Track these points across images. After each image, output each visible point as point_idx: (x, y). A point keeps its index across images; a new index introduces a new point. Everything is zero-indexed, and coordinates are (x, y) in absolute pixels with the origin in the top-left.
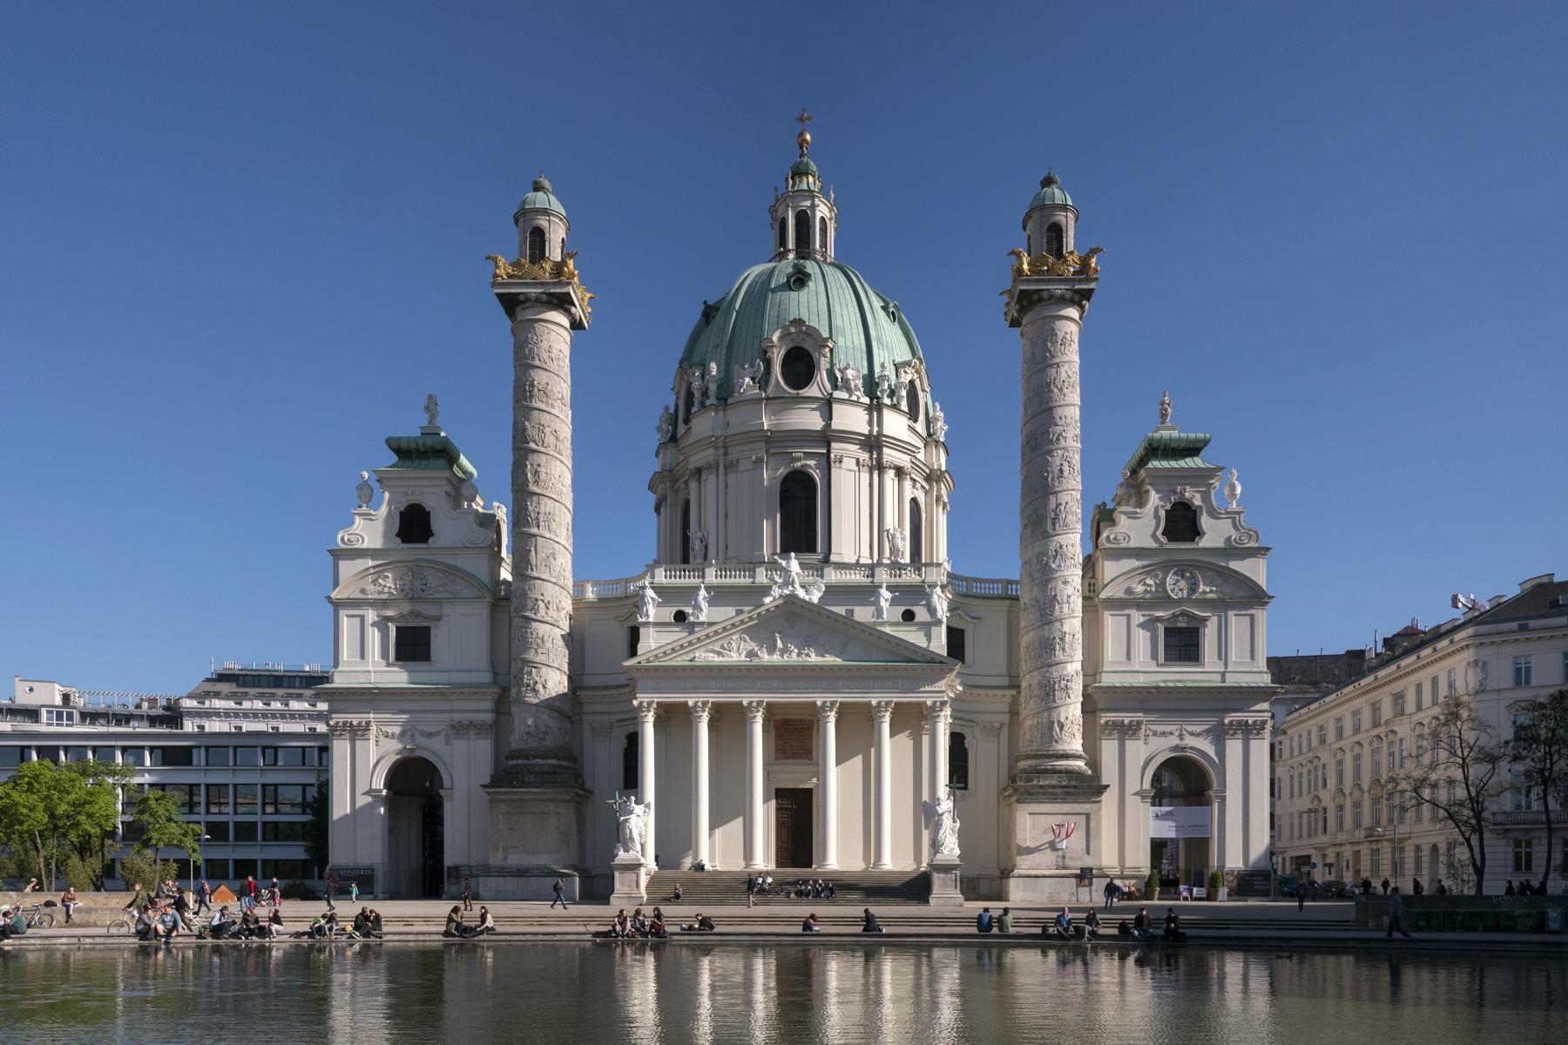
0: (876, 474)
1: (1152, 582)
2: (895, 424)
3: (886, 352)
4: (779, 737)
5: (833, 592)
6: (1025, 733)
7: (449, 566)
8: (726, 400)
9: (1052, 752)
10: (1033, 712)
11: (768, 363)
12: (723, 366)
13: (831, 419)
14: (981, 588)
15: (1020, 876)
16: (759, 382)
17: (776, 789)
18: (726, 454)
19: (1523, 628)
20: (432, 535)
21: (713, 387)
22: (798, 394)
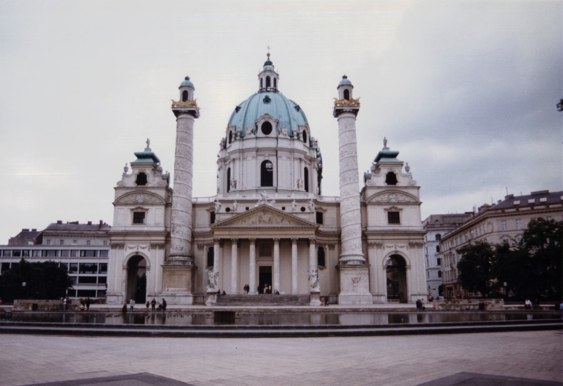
2: (299, 145)
5: (278, 201)
8: (243, 137)
11: (257, 127)
12: (242, 127)
13: (277, 143)
18: (243, 155)
21: (239, 134)
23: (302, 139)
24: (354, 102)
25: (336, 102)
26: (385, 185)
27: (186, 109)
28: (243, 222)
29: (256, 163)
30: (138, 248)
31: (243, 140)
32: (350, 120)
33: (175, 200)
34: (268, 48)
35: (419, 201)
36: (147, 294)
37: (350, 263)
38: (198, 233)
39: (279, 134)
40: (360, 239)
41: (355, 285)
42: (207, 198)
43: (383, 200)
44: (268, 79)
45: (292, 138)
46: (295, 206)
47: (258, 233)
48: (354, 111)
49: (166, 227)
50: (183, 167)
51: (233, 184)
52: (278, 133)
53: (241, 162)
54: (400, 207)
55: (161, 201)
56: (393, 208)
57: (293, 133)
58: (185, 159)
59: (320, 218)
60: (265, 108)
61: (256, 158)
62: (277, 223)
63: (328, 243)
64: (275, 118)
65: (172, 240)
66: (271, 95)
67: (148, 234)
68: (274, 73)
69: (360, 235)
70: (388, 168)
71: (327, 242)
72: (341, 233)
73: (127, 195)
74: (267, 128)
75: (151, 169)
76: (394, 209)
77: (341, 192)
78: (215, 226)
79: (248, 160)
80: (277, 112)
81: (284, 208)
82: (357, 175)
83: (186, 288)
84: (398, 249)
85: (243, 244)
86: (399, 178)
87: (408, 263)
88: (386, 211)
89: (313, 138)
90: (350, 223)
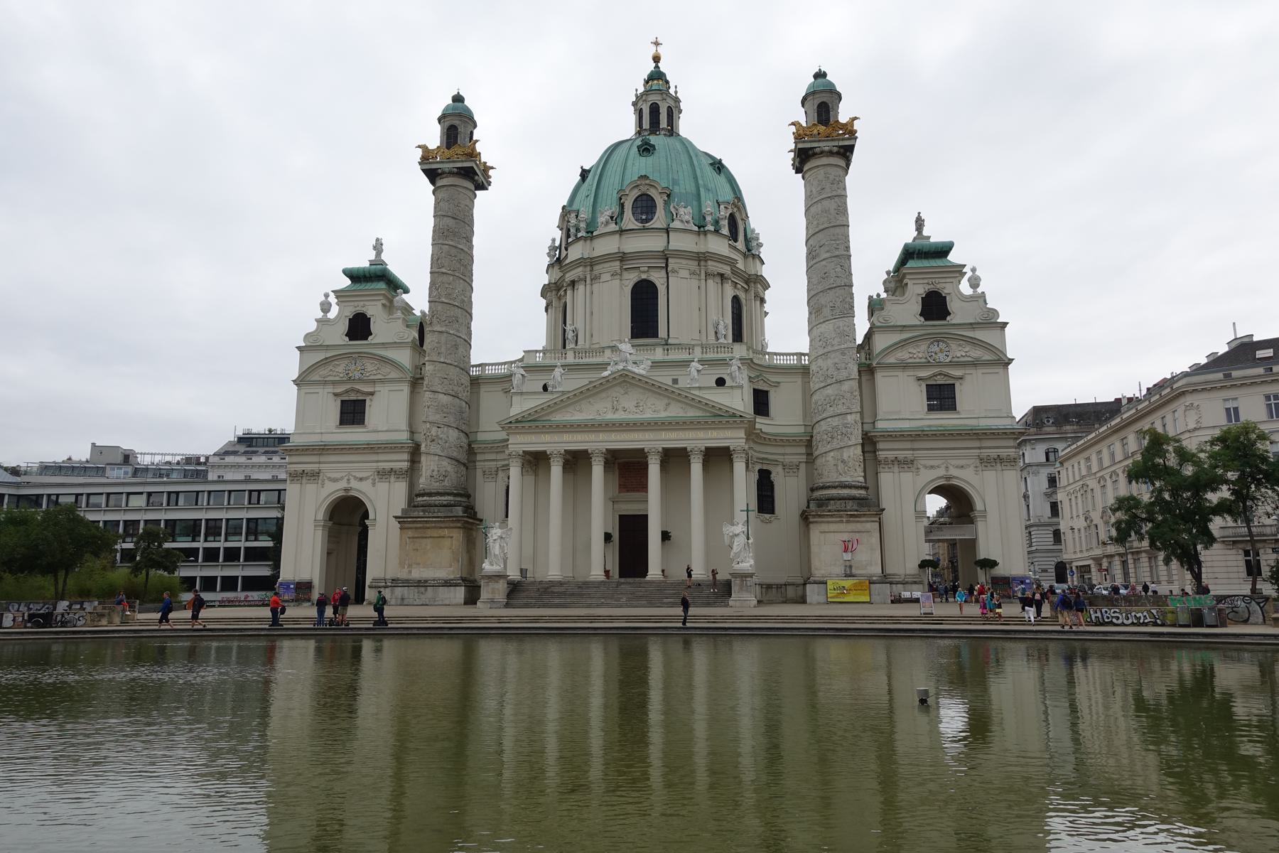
2: (718, 245)
3: (711, 195)
4: (621, 476)
7: (382, 357)
8: (592, 233)
9: (837, 484)
10: (823, 452)
11: (622, 206)
13: (669, 243)
14: (780, 360)
15: (815, 583)
16: (616, 219)
17: (620, 515)
18: (592, 270)
20: (371, 334)
22: (644, 226)
23: (725, 231)
24: (841, 129)
25: (798, 130)
27: (451, 165)
29: (621, 287)
30: (348, 480)
31: (592, 238)
32: (834, 172)
33: (429, 368)
34: (657, 44)
35: (1006, 356)
36: (368, 583)
38: (484, 442)
39: (673, 220)
40: (859, 448)
41: (847, 556)
42: (505, 363)
43: (915, 356)
44: (655, 110)
45: (702, 229)
46: (698, 371)
48: (842, 150)
49: (412, 433)
50: (448, 295)
52: (670, 220)
55: (402, 375)
56: (940, 374)
57: (704, 218)
58: (451, 278)
59: (761, 403)
60: (642, 165)
61: (621, 275)
62: (655, 409)
63: (782, 460)
64: (664, 185)
65: (423, 458)
66: (653, 139)
67: (371, 448)
68: (668, 94)
69: (857, 438)
70: (926, 281)
71: (780, 458)
72: (812, 437)
73: (326, 362)
74: (645, 206)
75: (379, 304)
76: (943, 377)
77: (811, 341)
78: (511, 422)
80: (668, 173)
81: (675, 381)
82: (847, 300)
83: (451, 566)
84: (953, 472)
85: (576, 462)
86: (952, 305)
87: (979, 506)
88: (920, 381)
89: (753, 231)
90: (830, 411)
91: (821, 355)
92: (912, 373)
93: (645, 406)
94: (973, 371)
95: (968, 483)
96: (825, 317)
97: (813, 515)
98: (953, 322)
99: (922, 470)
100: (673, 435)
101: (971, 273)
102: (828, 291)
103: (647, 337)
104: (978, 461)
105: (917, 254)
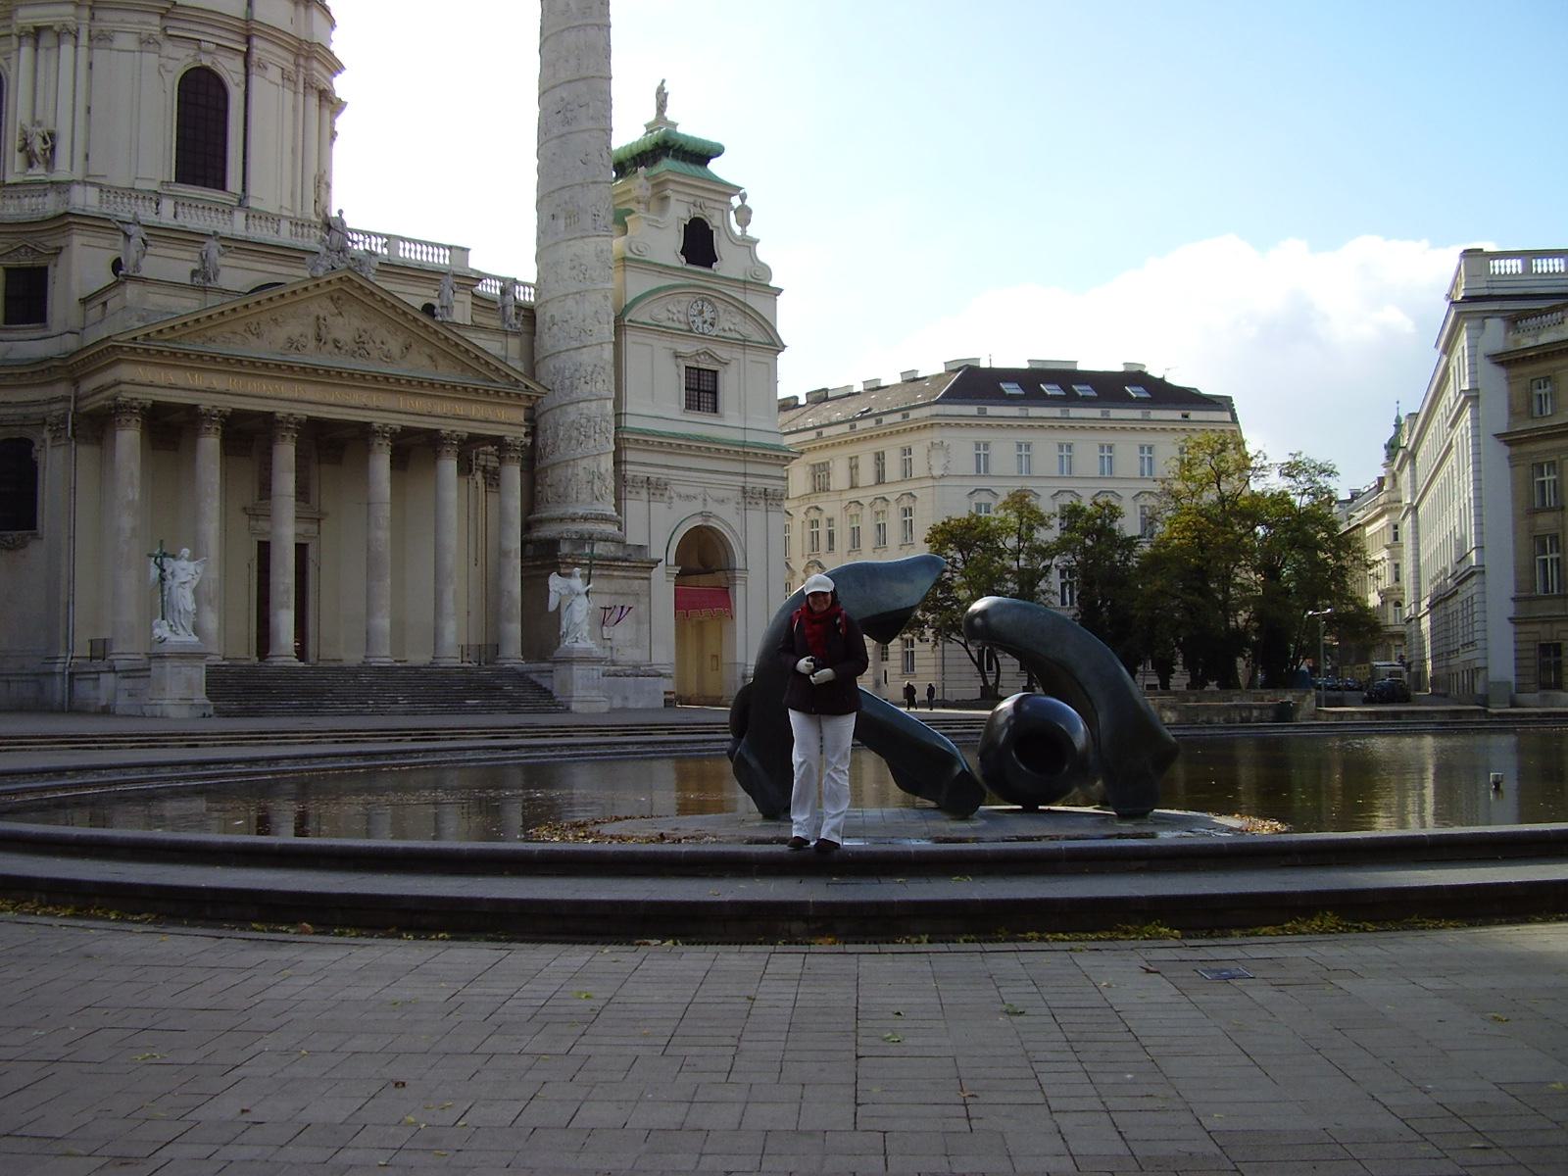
0: (301, 97)
1: (675, 311)
6: (550, 486)
10: (567, 458)
19: (982, 415)
26: (680, 261)
28: (250, 336)
29: (160, 72)
37: (600, 549)
40: (612, 455)
43: (675, 318)
47: (312, 393)
51: (38, 146)
53: (83, 52)
54: (722, 352)
70: (691, 200)
78: (135, 339)
79: (118, 50)
84: (712, 507)
86: (721, 245)
87: (739, 563)
88: (679, 360)
90: (584, 390)
91: (577, 293)
92: (669, 345)
93: (371, 344)
94: (740, 356)
95: (729, 526)
96: (584, 230)
97: (567, 563)
98: (719, 273)
99: (676, 499)
100: (419, 404)
101: (740, 203)
102: (591, 186)
103: (205, 186)
104: (740, 494)
105: (674, 151)
